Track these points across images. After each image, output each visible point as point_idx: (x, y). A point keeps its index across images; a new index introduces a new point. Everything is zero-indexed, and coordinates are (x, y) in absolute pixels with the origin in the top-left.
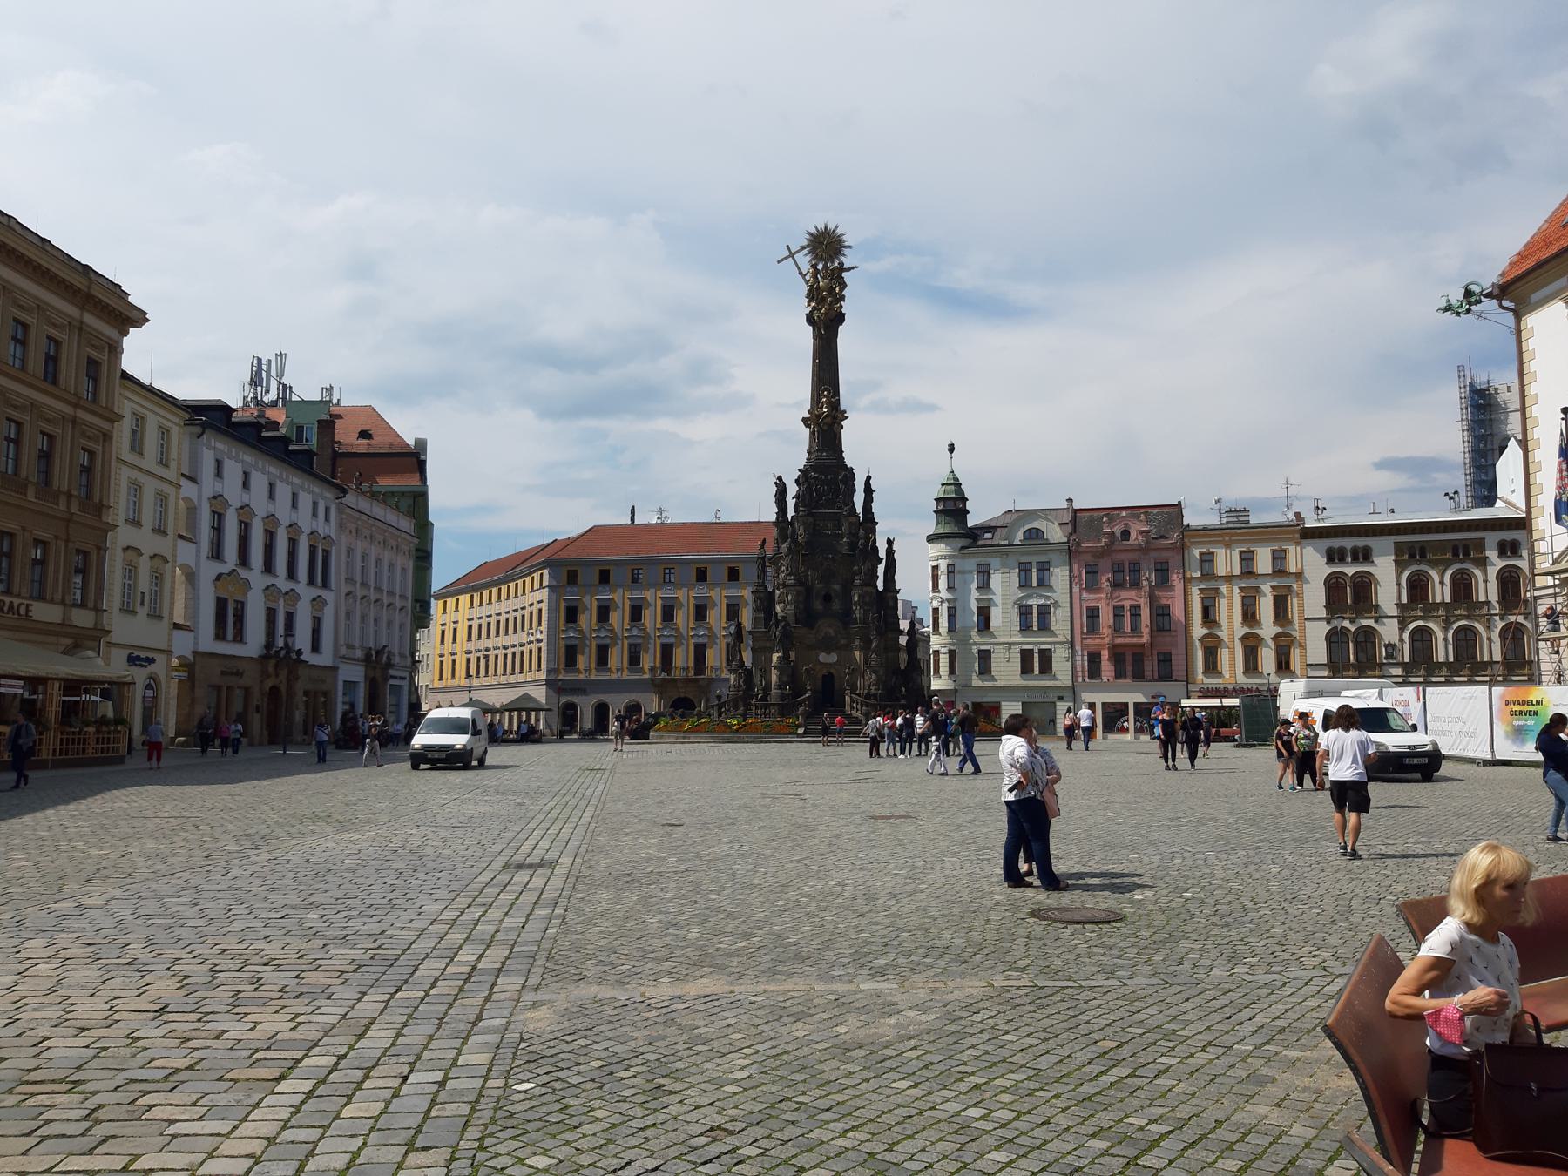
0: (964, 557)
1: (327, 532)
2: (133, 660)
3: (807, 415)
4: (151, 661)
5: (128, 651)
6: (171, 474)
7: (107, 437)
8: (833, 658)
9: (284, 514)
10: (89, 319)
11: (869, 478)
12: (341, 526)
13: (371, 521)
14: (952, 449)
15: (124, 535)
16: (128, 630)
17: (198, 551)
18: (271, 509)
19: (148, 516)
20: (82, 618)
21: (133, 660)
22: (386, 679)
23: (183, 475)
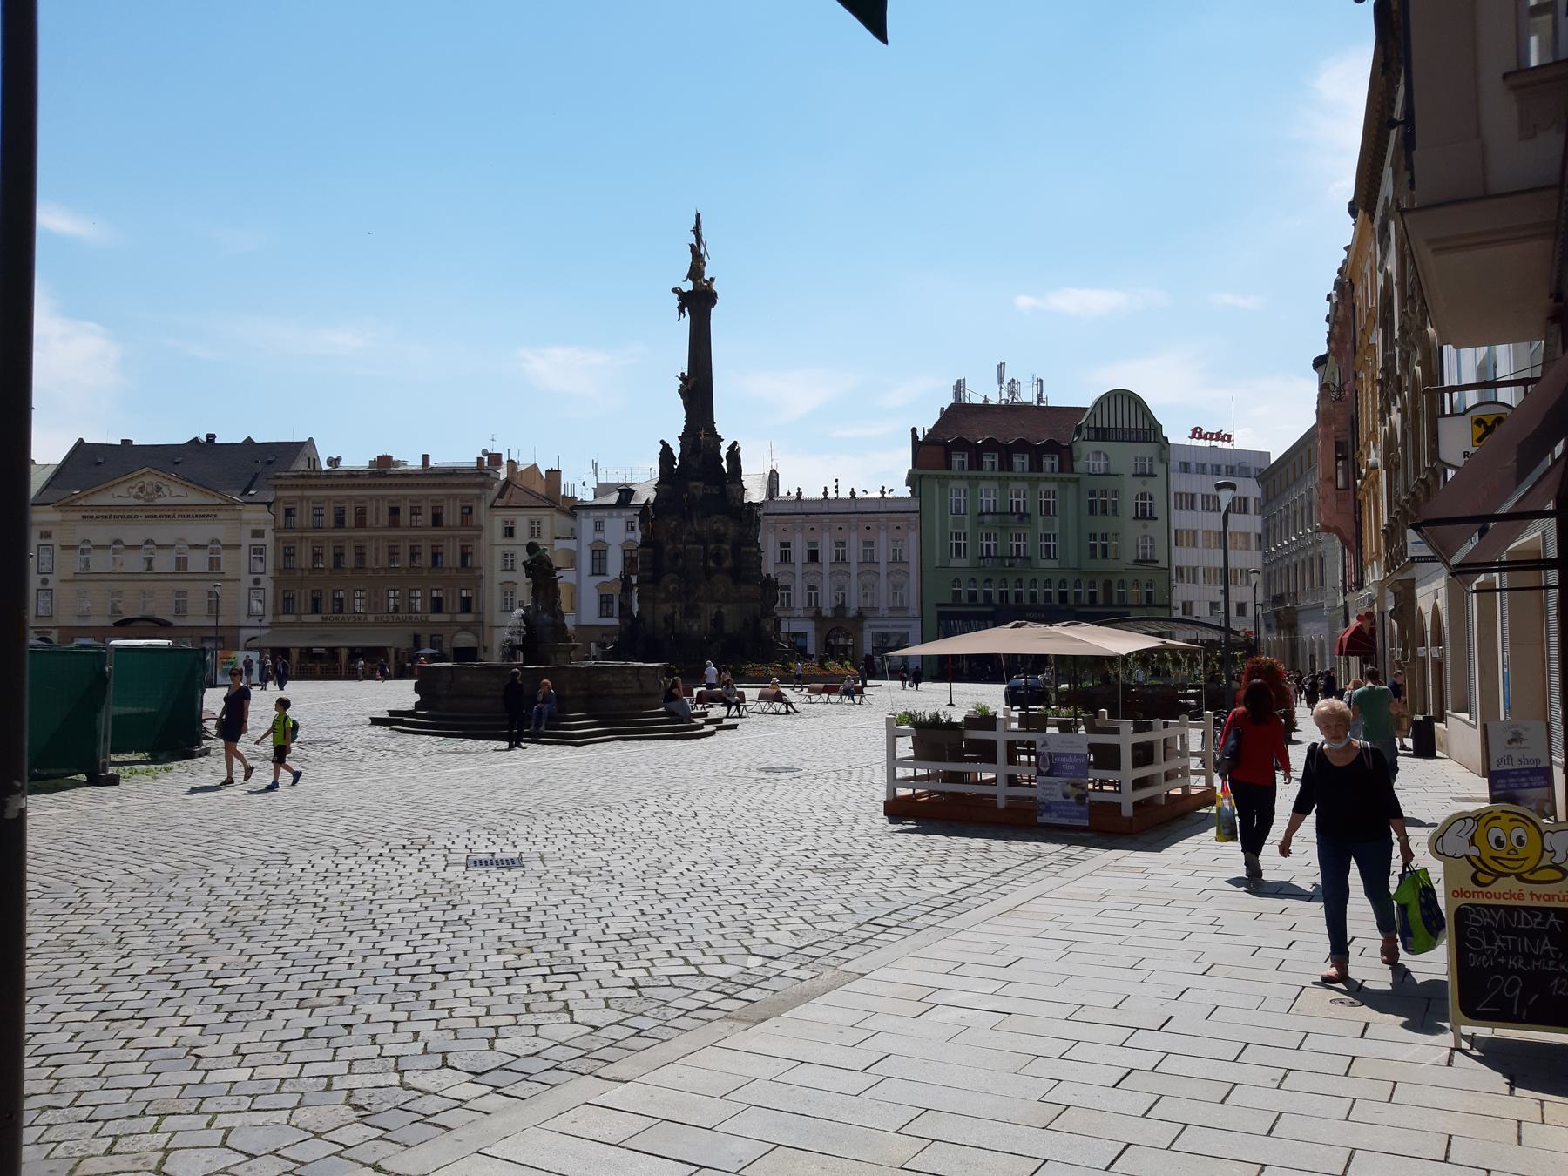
7: (478, 537)
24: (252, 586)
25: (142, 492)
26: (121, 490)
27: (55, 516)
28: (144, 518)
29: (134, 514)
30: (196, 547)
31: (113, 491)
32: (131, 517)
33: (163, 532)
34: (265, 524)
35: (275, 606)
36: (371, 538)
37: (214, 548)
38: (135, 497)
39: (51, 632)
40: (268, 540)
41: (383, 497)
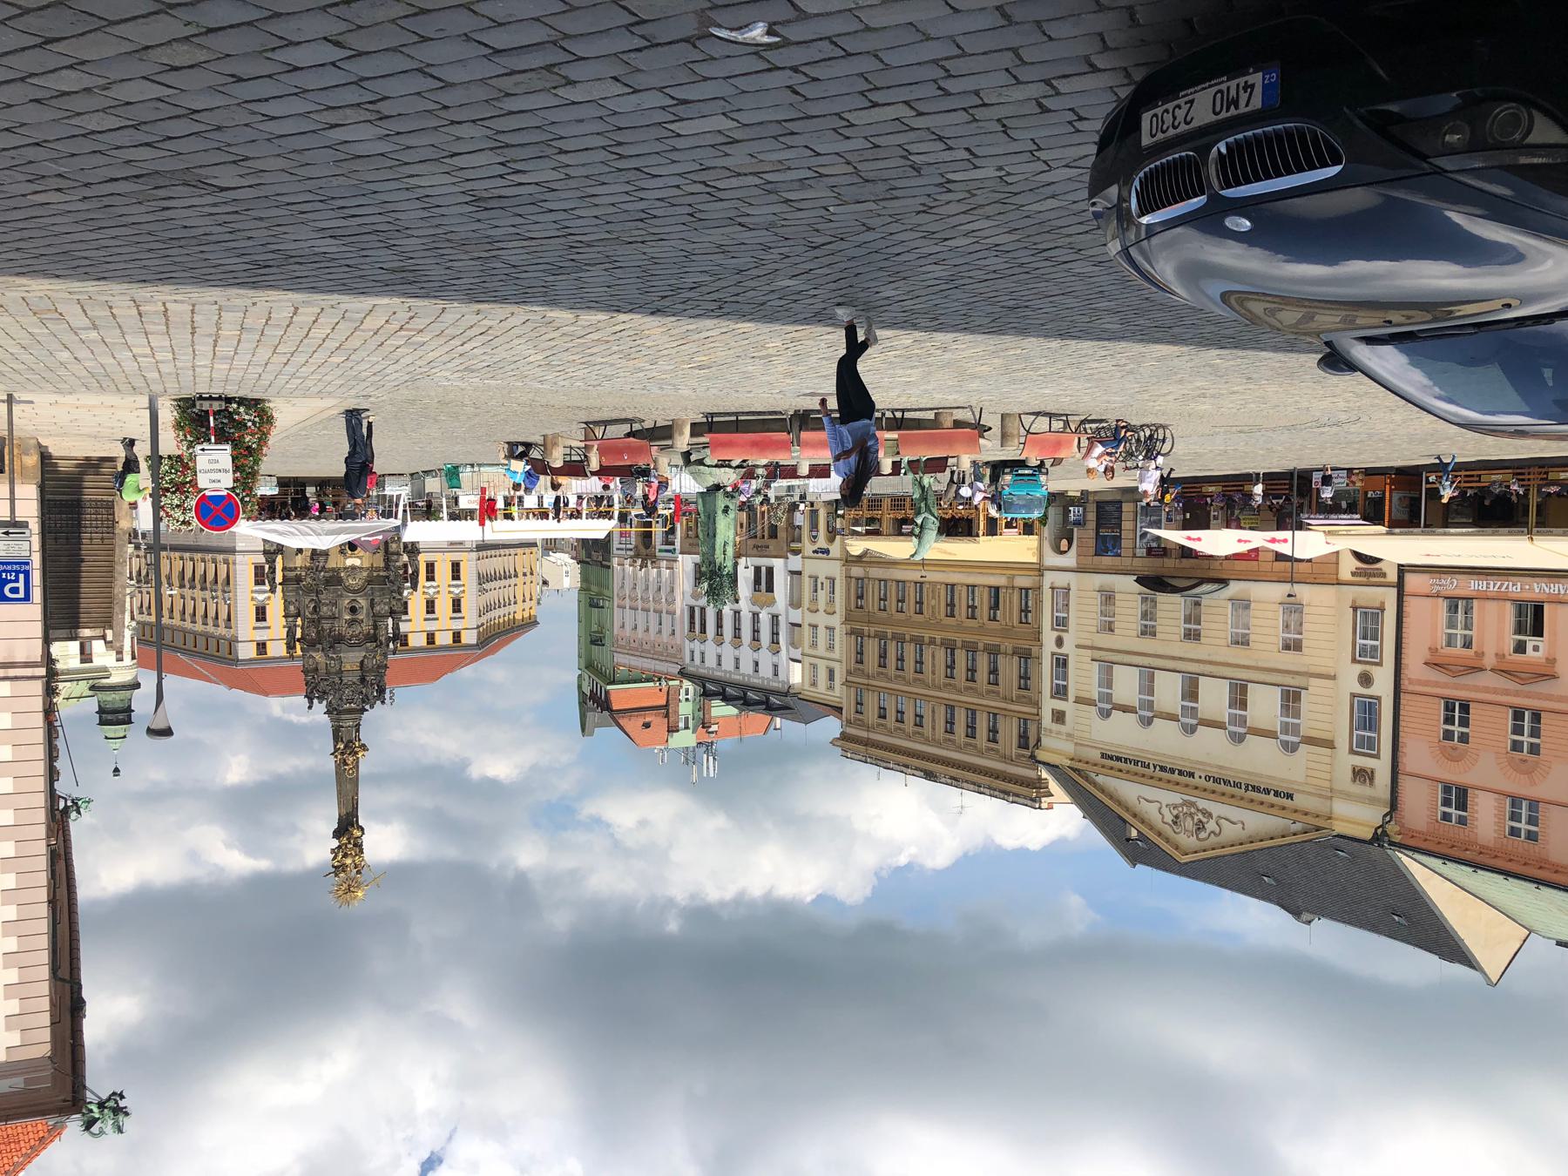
0: (105, 669)
1: (692, 645)
2: (827, 552)
3: (365, 753)
4: (814, 552)
5: (830, 556)
6: (807, 660)
7: (849, 673)
8: (349, 562)
9: (728, 651)
10: (864, 734)
11: (310, 707)
12: (680, 650)
13: (656, 657)
14: (116, 770)
15: (836, 621)
16: (835, 569)
17: (787, 618)
18: (737, 652)
19: (822, 634)
20: (857, 571)
21: (827, 552)
22: (636, 547)
23: (799, 661)
24: (1064, 635)
25: (1201, 821)
26: (1230, 832)
27: (1341, 808)
28: (1196, 776)
29: (1210, 785)
30: (1126, 709)
31: (1243, 835)
32: (1216, 780)
33: (1164, 741)
34: (1051, 731)
35: (1039, 602)
36: (939, 689)
37: (1108, 707)
38: (1210, 815)
39: (1353, 574)
40: (1049, 705)
41: (927, 741)
